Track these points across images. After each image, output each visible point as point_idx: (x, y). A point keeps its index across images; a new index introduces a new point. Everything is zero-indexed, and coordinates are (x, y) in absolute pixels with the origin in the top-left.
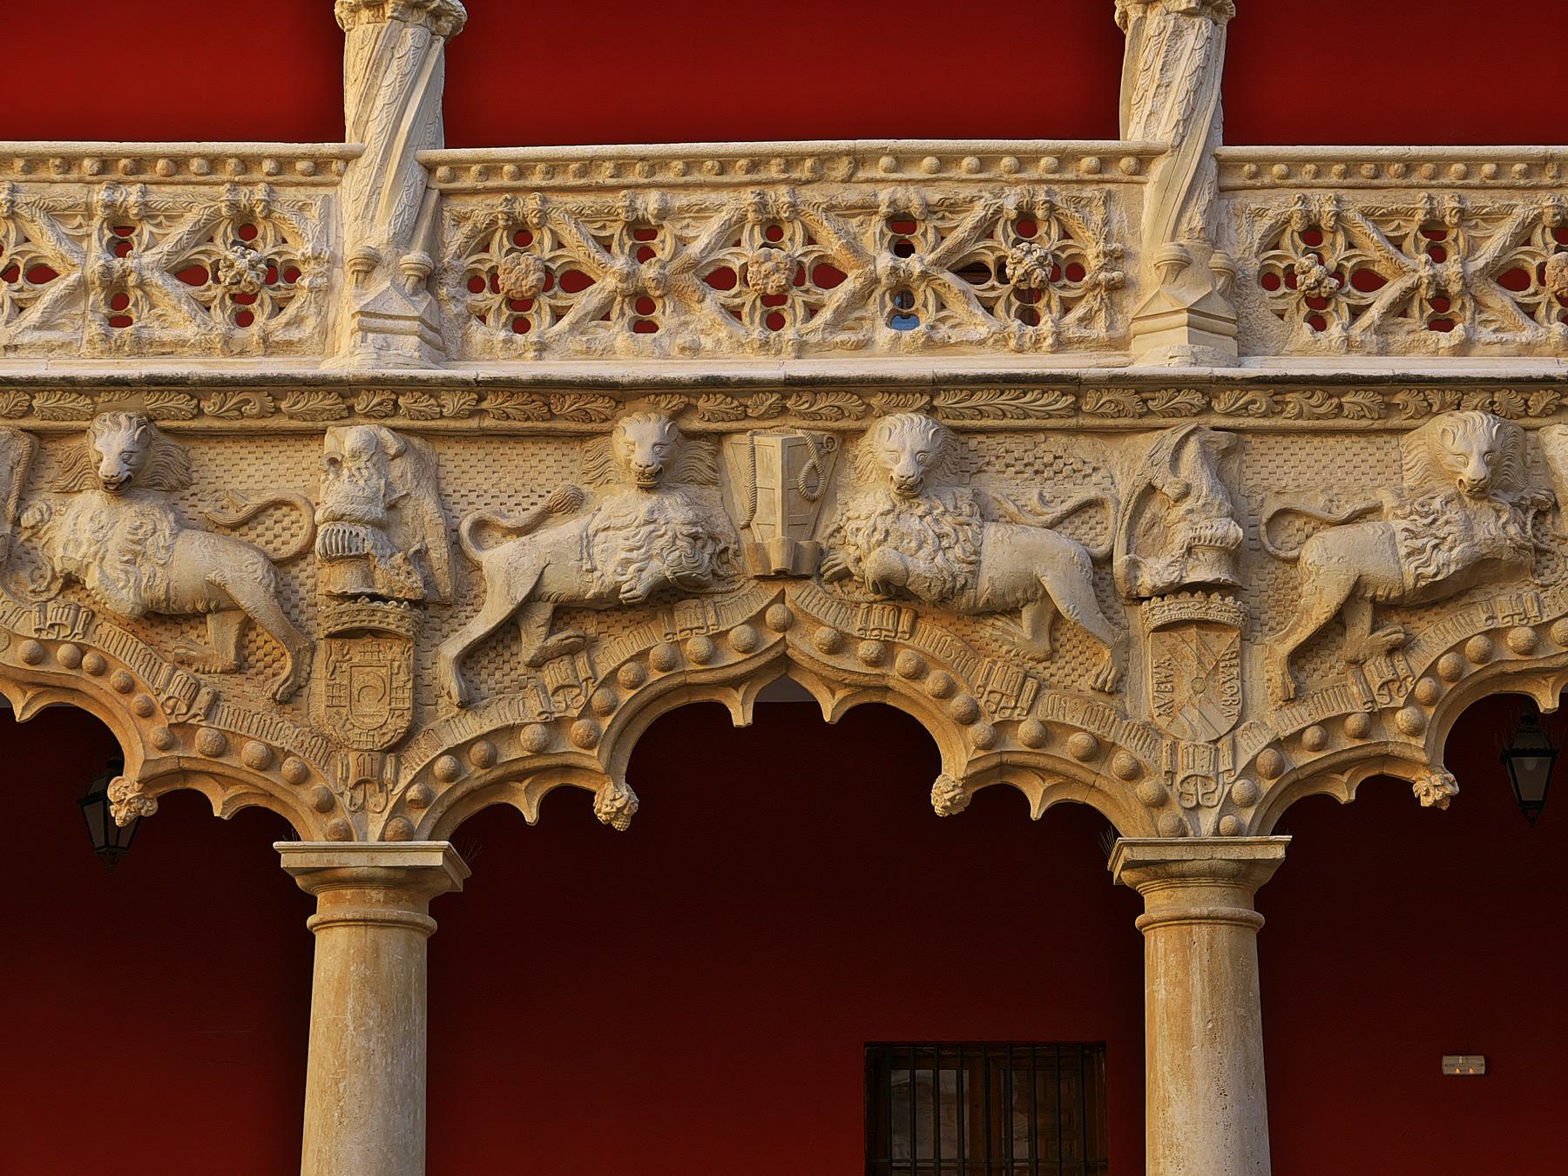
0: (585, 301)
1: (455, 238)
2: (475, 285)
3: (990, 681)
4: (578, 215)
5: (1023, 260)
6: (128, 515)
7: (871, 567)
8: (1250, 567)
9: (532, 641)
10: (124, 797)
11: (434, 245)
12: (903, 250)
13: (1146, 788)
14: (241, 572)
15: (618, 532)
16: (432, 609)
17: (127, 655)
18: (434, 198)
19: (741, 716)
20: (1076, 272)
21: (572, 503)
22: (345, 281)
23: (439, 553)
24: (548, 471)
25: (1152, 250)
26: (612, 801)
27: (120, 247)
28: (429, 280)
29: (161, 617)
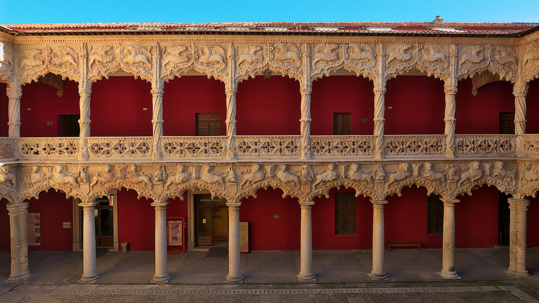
0: (324, 150)
1: (312, 144)
2: (314, 148)
3: (362, 187)
4: (323, 142)
5: (365, 147)
6: (285, 173)
7: (352, 178)
8: (386, 178)
9: (321, 184)
10: (284, 196)
11: (310, 145)
12: (354, 145)
13: (375, 196)
14: (295, 179)
15: (328, 174)
16: (312, 182)
17: (285, 185)
18: (310, 140)
19: (339, 189)
20: (370, 147)
21: (325, 171)
22: (303, 150)
23: (313, 176)
24: (322, 169)
25: (377, 147)
26: (327, 196)
27: (281, 145)
28: (310, 148)
29: (288, 182)
